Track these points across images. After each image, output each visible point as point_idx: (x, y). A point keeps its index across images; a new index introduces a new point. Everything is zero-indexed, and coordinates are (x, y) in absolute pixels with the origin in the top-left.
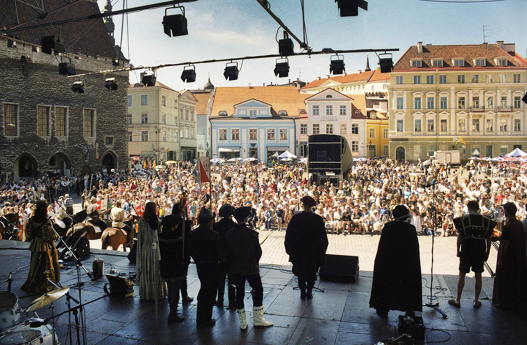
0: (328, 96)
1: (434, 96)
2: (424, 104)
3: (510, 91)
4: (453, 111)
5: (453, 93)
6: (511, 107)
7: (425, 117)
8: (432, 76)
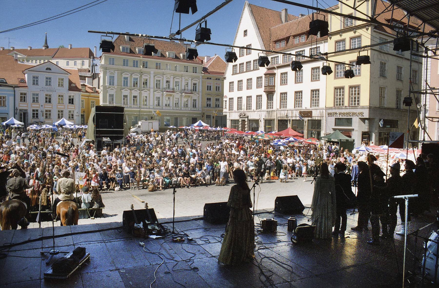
0: (47, 69)
2: (130, 83)
3: (190, 78)
4: (152, 90)
5: (152, 76)
6: (191, 90)
7: (131, 93)
8: (137, 61)
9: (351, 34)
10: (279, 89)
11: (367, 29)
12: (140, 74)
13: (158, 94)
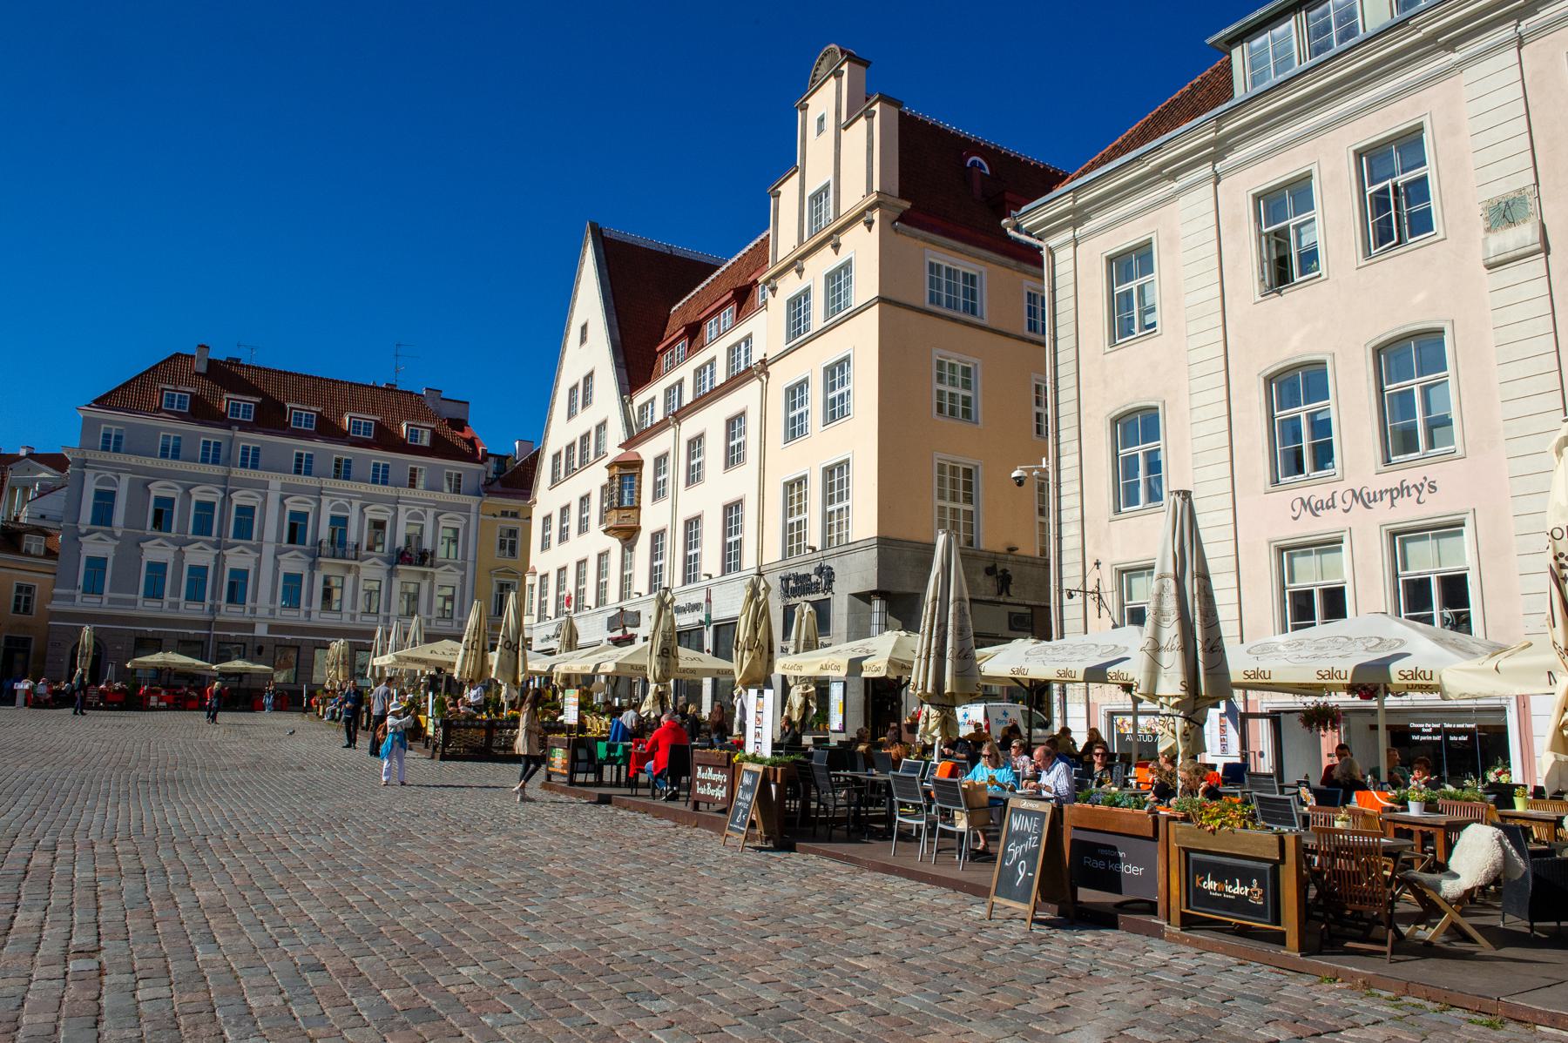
1: (215, 497)
4: (269, 550)
5: (274, 497)
10: (652, 516)
11: (869, 224)
12: (224, 491)
13: (293, 563)
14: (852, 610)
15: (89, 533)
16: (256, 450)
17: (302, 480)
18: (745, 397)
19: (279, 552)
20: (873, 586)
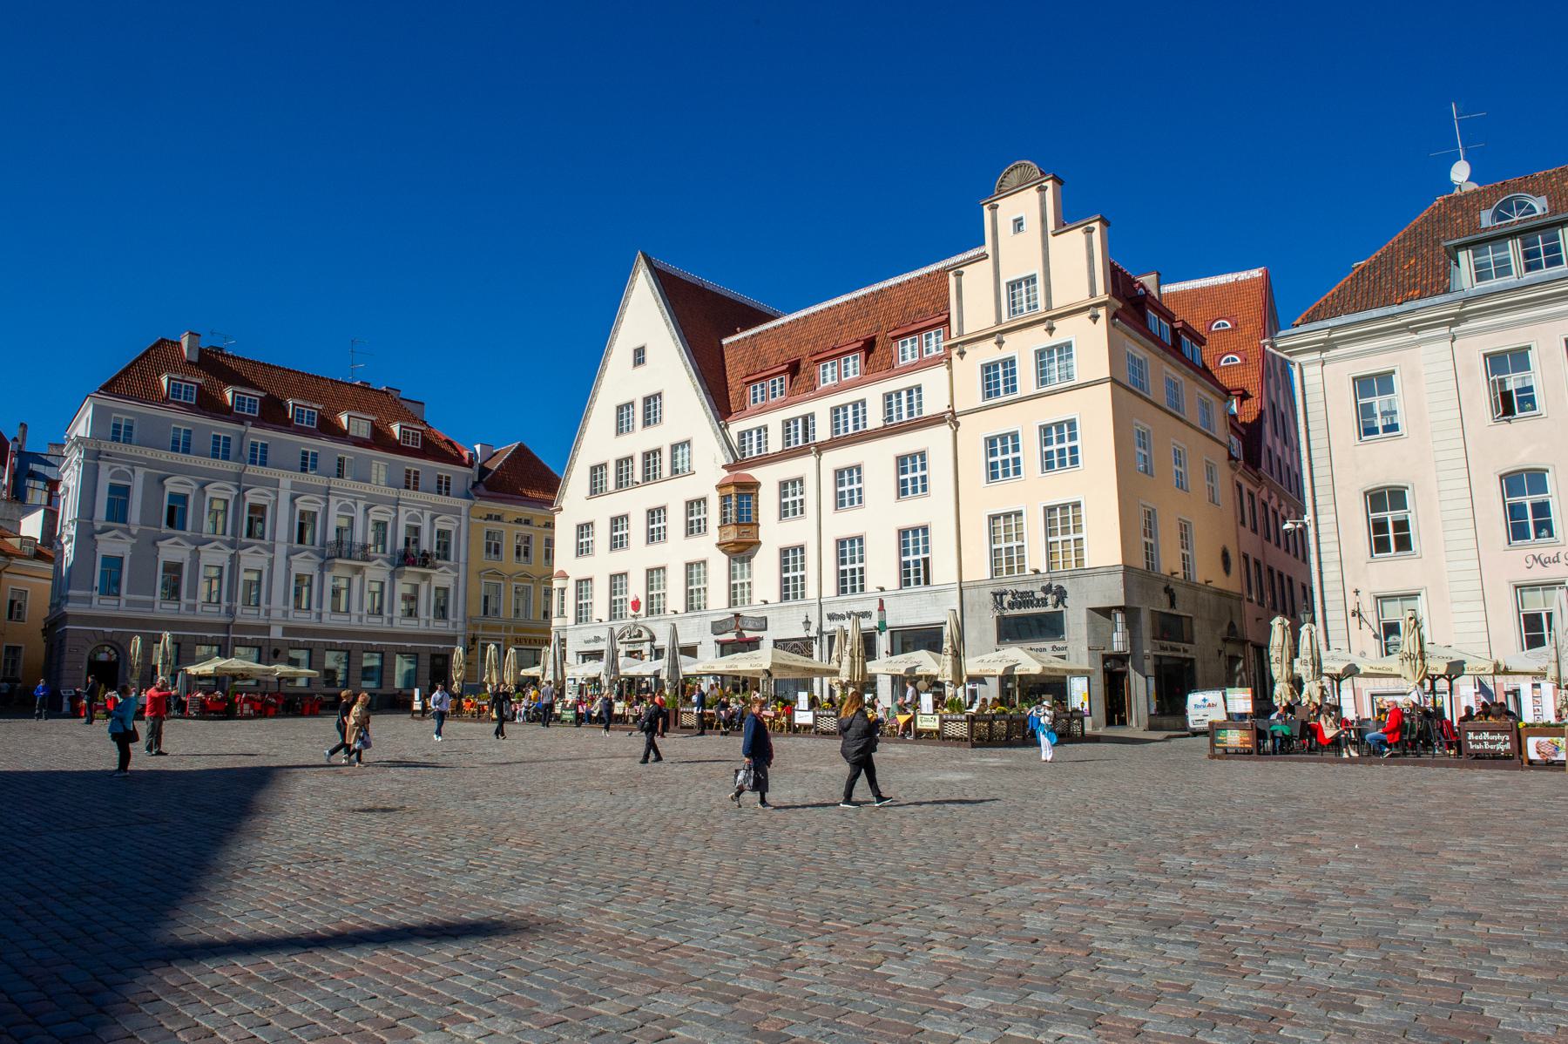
4: (281, 550)
9: (1038, 338)
10: (773, 533)
11: (1095, 318)
12: (238, 488)
13: (304, 565)
14: (1091, 623)
15: (104, 530)
16: (265, 446)
17: (311, 478)
18: (934, 441)
19: (291, 553)
20: (1122, 603)
